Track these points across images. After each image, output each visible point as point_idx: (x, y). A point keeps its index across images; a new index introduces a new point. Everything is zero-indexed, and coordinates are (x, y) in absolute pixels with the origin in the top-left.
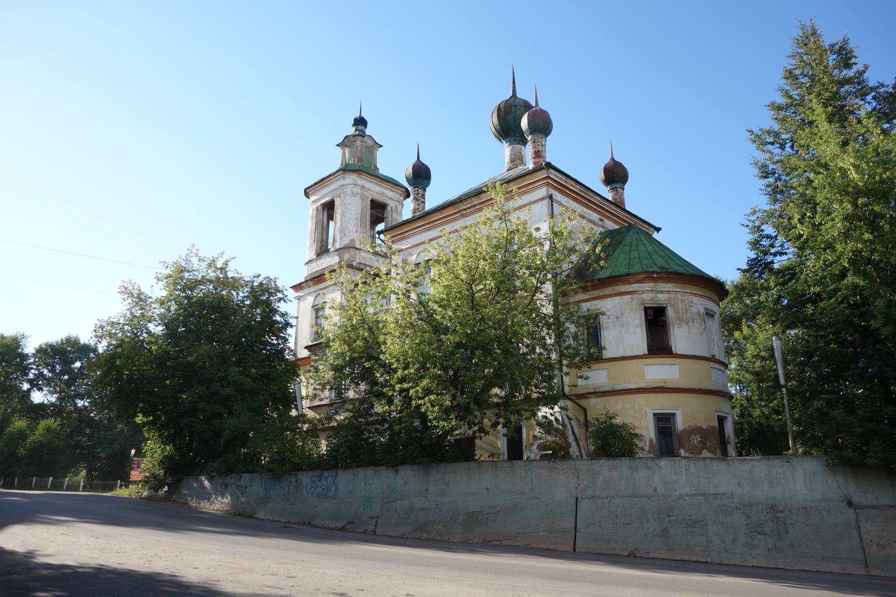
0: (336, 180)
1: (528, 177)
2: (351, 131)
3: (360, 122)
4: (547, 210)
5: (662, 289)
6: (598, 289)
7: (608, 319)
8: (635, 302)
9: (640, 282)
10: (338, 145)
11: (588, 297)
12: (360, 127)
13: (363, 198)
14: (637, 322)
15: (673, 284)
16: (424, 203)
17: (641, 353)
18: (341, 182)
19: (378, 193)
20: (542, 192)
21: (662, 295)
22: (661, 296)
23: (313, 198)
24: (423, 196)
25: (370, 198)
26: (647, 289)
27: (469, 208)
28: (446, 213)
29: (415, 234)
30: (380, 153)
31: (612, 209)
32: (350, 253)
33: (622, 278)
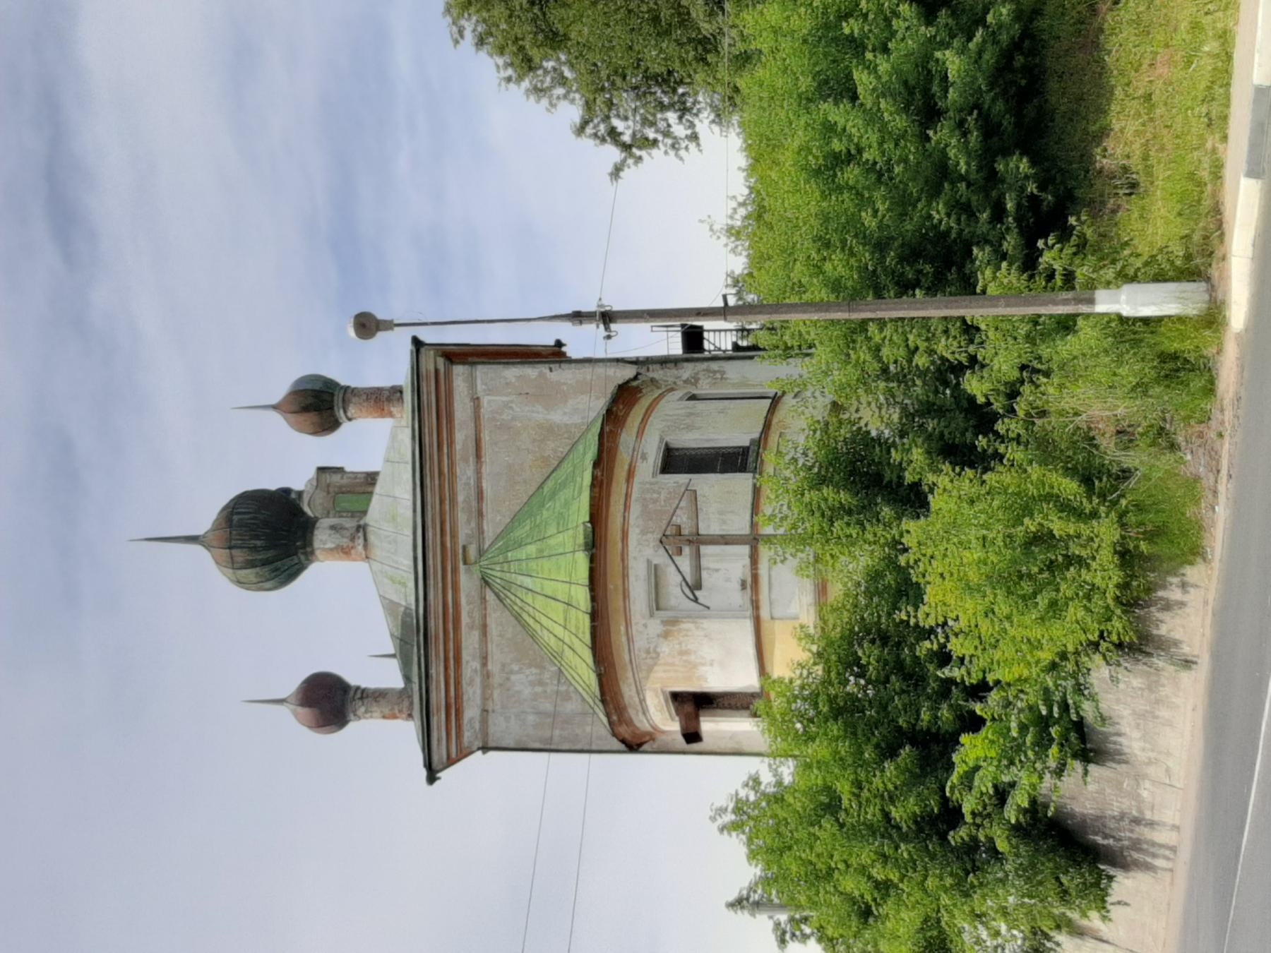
15: (621, 683)
31: (435, 535)
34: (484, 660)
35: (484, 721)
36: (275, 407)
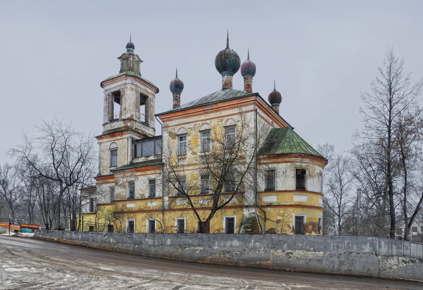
0: (121, 80)
1: (245, 98)
2: (125, 51)
3: (130, 46)
4: (254, 117)
5: (305, 161)
6: (275, 158)
8: (293, 166)
9: (296, 157)
10: (118, 58)
11: (271, 162)
12: (131, 49)
13: (137, 92)
14: (293, 175)
16: (179, 101)
17: (293, 190)
18: (124, 82)
19: (144, 90)
20: (252, 107)
22: (303, 165)
23: (107, 88)
24: (179, 97)
25: (140, 92)
26: (298, 161)
27: (210, 109)
28: (196, 110)
29: (177, 119)
30: (141, 65)
32: (131, 123)
36: (275, 89)
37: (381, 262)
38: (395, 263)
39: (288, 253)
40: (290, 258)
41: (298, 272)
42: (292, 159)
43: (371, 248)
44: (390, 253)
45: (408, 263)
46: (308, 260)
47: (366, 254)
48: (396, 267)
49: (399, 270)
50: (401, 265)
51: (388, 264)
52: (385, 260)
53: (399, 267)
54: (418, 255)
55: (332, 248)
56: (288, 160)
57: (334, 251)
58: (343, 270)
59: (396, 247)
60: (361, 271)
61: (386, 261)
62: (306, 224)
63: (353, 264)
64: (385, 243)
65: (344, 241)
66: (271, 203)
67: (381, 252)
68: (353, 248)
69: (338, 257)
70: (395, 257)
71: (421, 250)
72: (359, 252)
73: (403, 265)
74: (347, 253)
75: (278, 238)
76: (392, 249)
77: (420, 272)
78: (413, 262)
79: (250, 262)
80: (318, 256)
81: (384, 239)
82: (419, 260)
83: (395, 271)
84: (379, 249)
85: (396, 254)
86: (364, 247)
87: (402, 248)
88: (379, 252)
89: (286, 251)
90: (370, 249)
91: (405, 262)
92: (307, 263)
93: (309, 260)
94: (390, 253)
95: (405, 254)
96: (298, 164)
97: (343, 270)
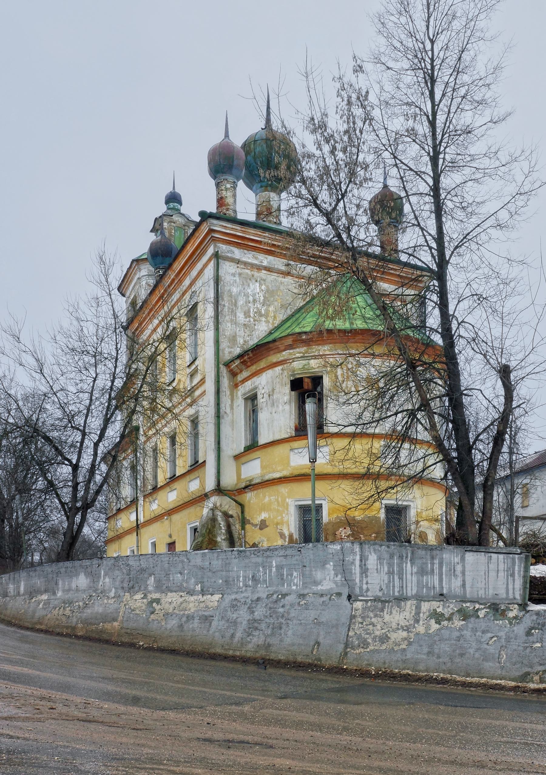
7: (263, 398)
9: (290, 347)
14: (286, 398)
21: (316, 361)
22: (313, 363)
26: (298, 355)
33: (271, 345)
34: (268, 269)
35: (232, 260)
37: (360, 620)
38: (403, 623)
39: (153, 601)
40: (152, 613)
41: (162, 650)
42: (284, 356)
43: (339, 576)
44: (397, 590)
45: (449, 619)
46: (184, 619)
47: (322, 595)
48: (405, 634)
49: (410, 644)
50: (421, 628)
51: (379, 627)
52: (371, 615)
53: (412, 635)
54: (491, 592)
55: (241, 584)
56: (275, 360)
57: (246, 590)
58: (250, 646)
59: (415, 570)
60: (296, 647)
61: (376, 616)
62: (328, 523)
63: (281, 628)
64: (379, 558)
65: (269, 560)
66: (250, 481)
67: (368, 590)
68: (292, 580)
69: (251, 610)
70: (409, 603)
71: (501, 574)
72: (305, 592)
73: (428, 628)
74: (275, 596)
75: (138, 564)
76: (401, 579)
77: (478, 649)
78: (465, 615)
79: (91, 624)
80: (207, 607)
81: (377, 547)
82: (489, 607)
83: (396, 648)
84: (361, 581)
85: (414, 592)
86: (319, 575)
87: (436, 571)
88: (361, 588)
89: (150, 596)
90: (335, 582)
91: (438, 617)
92: (181, 626)
93: (187, 617)
94: (397, 590)
95: (445, 592)
96: (297, 365)
97: (250, 646)
